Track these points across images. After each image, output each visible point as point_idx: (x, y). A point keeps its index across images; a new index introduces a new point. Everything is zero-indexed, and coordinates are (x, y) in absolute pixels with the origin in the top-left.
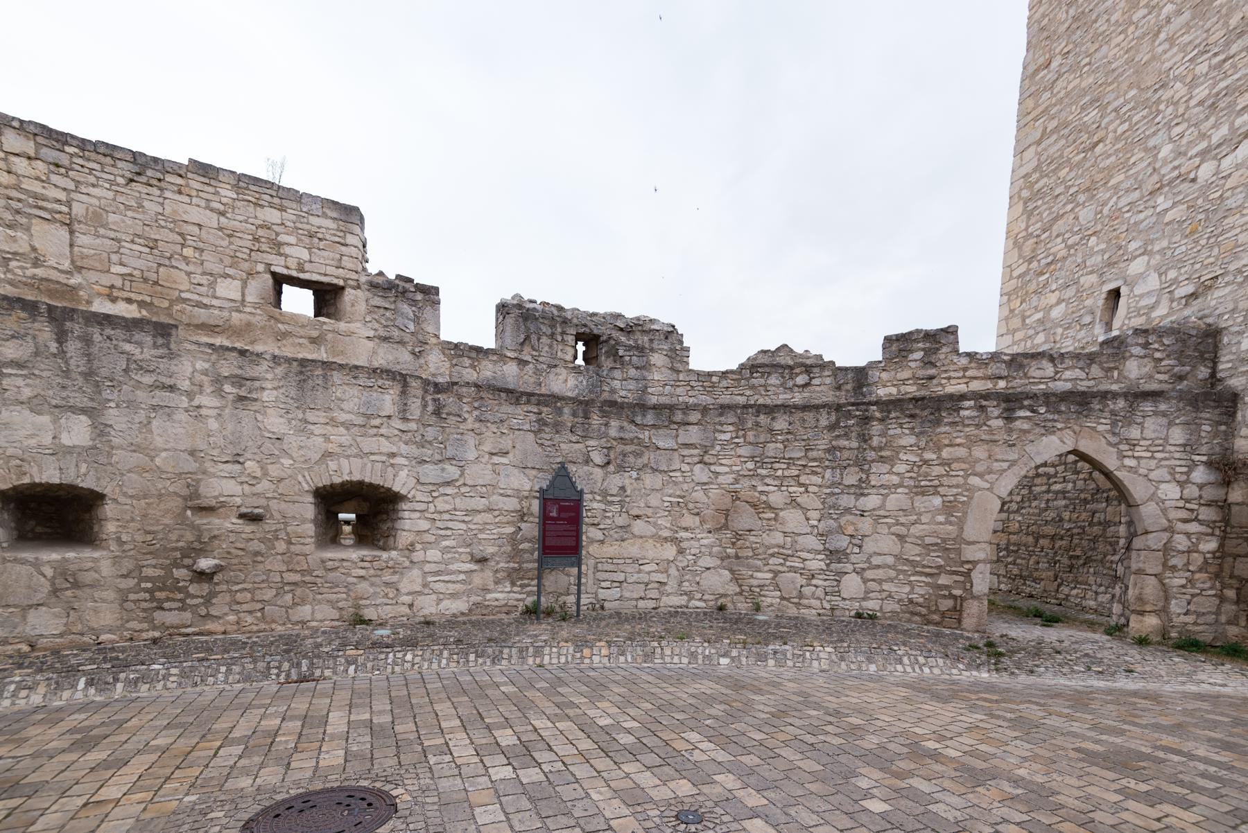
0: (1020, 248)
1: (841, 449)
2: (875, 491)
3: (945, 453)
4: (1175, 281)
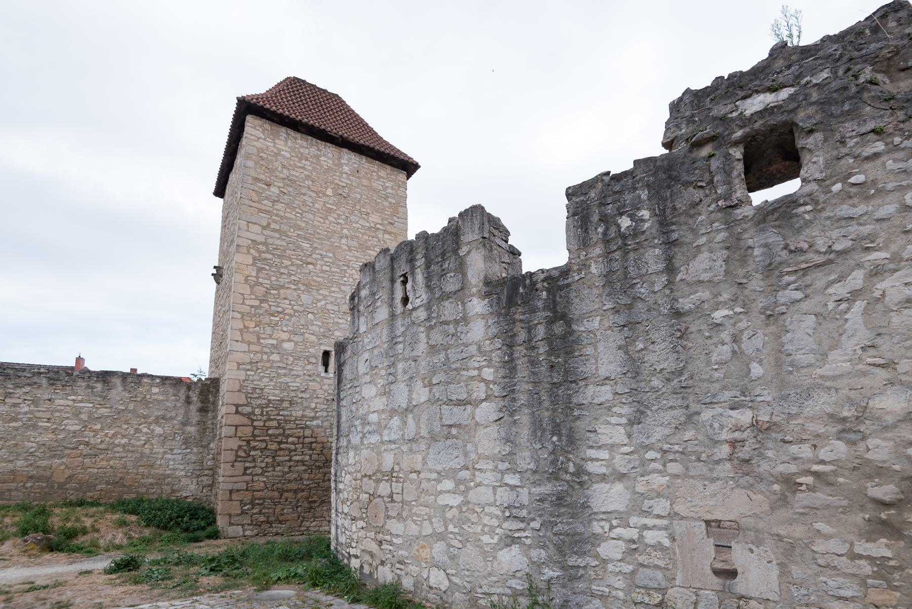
0: (252, 287)
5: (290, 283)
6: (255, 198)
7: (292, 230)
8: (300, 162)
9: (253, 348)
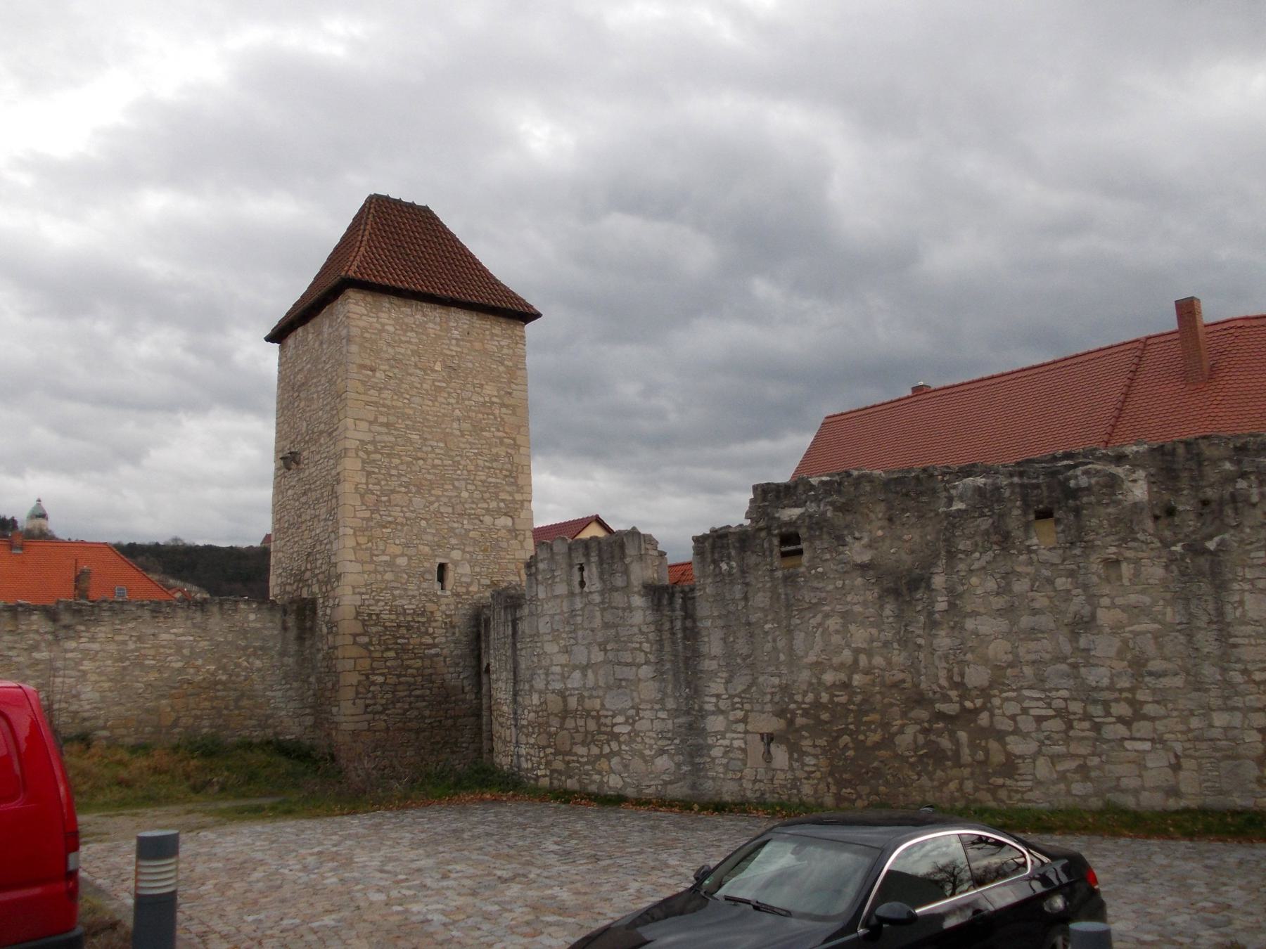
0: (362, 496)
4: (479, 574)
5: (401, 485)
6: (361, 389)
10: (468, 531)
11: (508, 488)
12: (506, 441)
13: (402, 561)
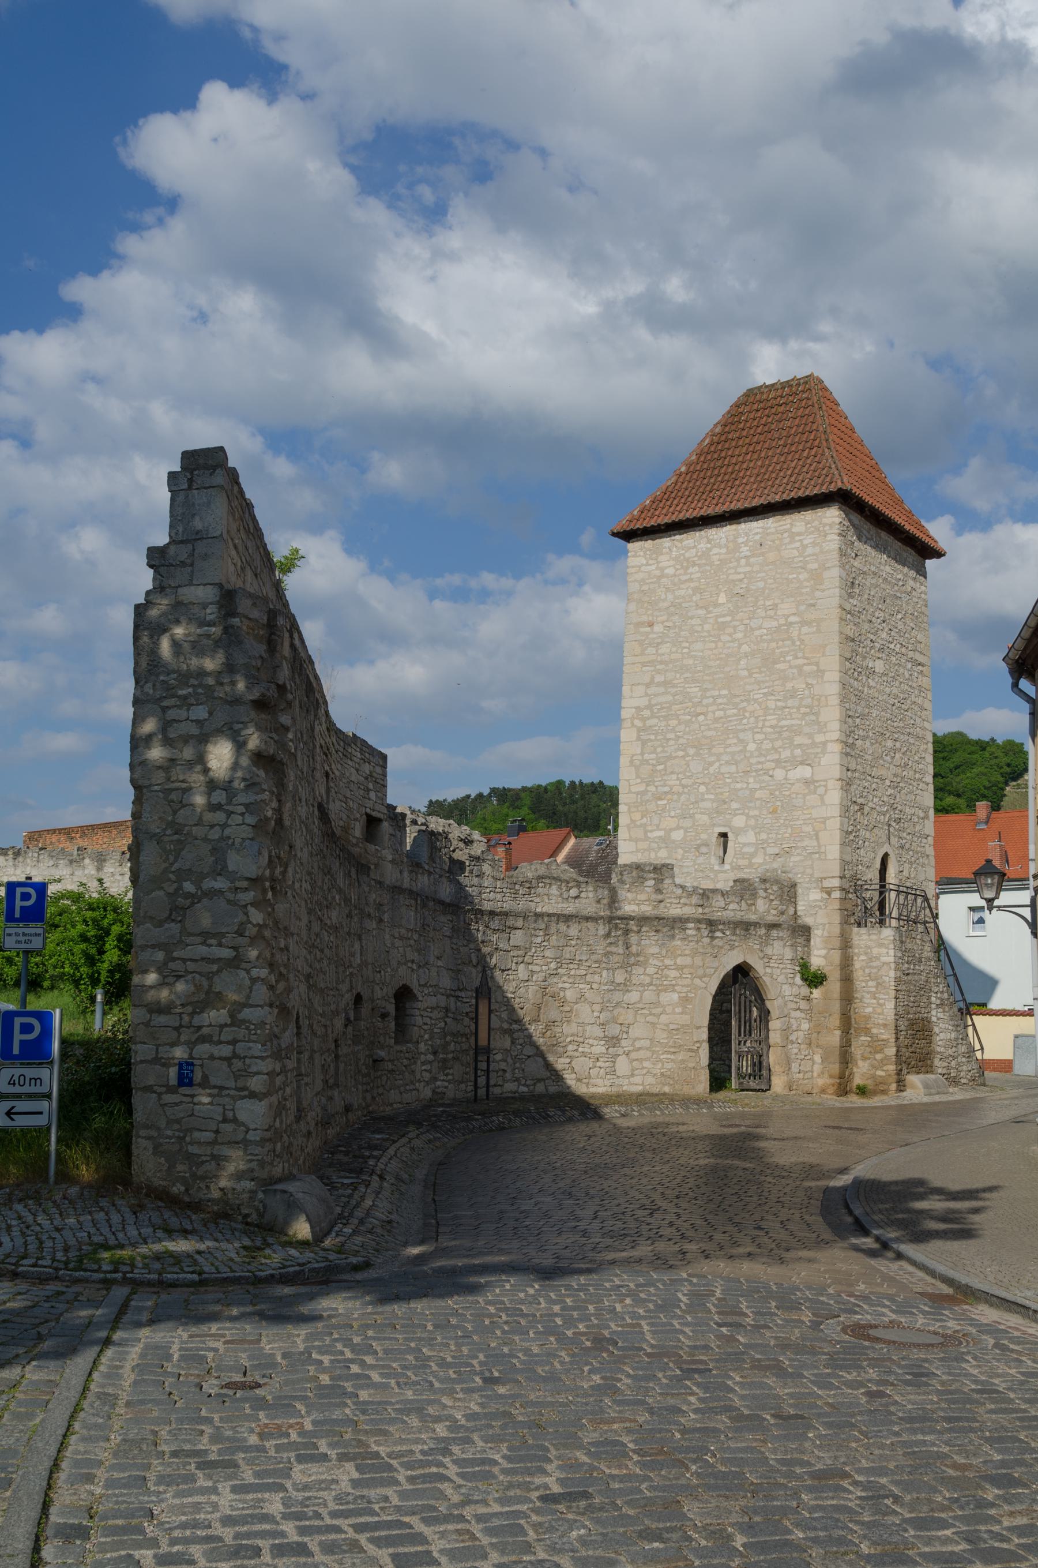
0: (637, 768)
1: (612, 953)
2: (635, 988)
3: (679, 961)
4: (764, 841)
7: (678, 676)
8: (686, 574)
9: (642, 845)
10: (753, 791)
11: (807, 730)
12: (807, 668)
13: (677, 835)
